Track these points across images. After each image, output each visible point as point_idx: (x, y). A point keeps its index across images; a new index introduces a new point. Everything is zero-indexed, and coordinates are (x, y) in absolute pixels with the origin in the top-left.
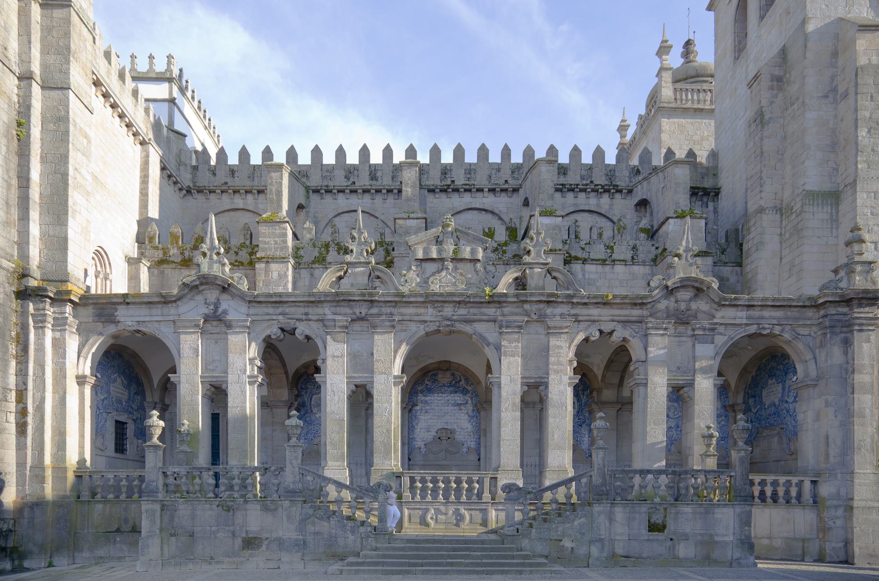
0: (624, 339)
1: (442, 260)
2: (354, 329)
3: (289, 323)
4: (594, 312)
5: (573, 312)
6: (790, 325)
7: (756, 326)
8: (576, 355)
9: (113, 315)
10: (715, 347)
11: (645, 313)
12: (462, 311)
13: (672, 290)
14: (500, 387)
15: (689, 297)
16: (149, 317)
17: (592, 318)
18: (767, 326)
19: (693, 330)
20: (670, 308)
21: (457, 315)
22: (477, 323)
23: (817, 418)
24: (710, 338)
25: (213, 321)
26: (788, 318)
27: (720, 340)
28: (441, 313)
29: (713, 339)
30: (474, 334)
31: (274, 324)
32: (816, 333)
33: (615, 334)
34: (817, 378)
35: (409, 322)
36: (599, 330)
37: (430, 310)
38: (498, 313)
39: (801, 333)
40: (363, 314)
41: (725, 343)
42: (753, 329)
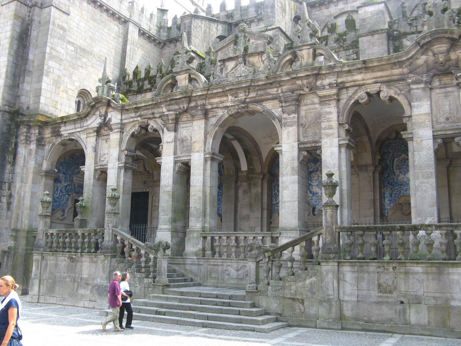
1: (237, 57)
2: (183, 120)
3: (144, 122)
4: (358, 77)
5: (340, 80)
9: (60, 132)
11: (405, 70)
12: (252, 95)
15: (446, 48)
16: (74, 130)
17: (357, 83)
20: (429, 62)
21: (249, 98)
25: (105, 127)
28: (237, 99)
30: (264, 111)
33: (382, 95)
35: (217, 110)
37: (230, 97)
38: (280, 91)
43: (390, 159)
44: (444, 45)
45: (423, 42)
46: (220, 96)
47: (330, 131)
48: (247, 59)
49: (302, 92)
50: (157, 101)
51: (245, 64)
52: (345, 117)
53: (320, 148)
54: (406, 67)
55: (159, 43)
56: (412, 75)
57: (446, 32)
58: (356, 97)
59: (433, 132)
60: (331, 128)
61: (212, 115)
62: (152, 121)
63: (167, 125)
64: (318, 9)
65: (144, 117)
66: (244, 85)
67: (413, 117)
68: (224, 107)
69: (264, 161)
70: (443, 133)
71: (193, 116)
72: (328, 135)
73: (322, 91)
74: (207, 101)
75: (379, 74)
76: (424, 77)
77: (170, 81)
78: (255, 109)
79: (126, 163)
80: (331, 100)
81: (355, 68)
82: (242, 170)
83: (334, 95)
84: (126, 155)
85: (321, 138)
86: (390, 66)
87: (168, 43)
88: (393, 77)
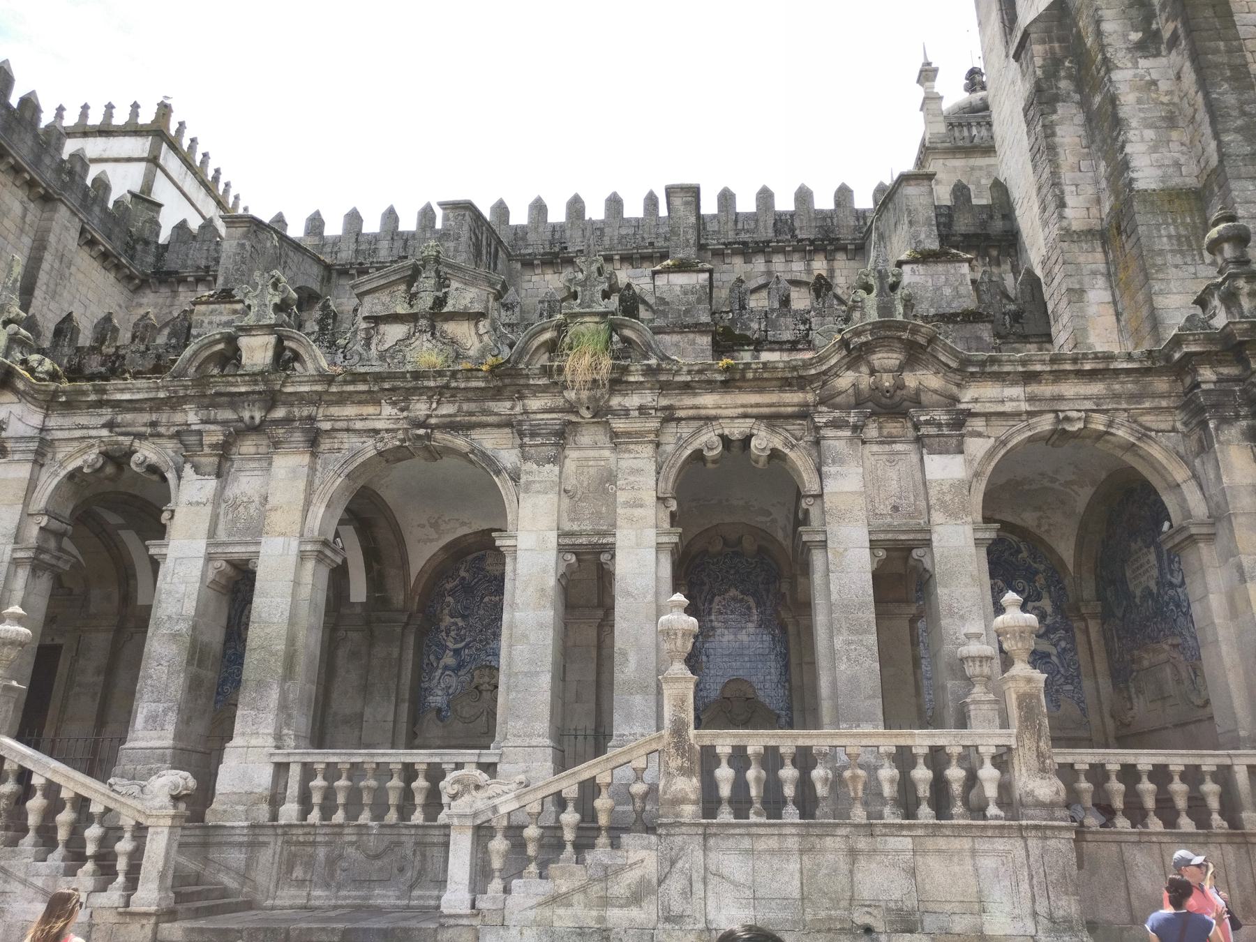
1: (412, 318)
2: (244, 449)
4: (708, 400)
5: (664, 402)
6: (1125, 410)
7: (1052, 416)
10: (969, 462)
11: (810, 397)
12: (447, 409)
14: (515, 559)
15: (898, 362)
17: (703, 412)
18: (1074, 414)
19: (916, 427)
20: (862, 387)
21: (437, 416)
22: (478, 431)
24: (954, 441)
26: (1116, 397)
27: (977, 447)
28: (405, 414)
30: (472, 452)
31: (93, 445)
32: (1185, 424)
33: (754, 442)
34: (1211, 520)
35: (345, 435)
36: (722, 436)
37: (388, 410)
38: (518, 409)
39: (1154, 426)
40: (257, 421)
41: (991, 453)
42: (1045, 424)
43: (703, 598)
44: (895, 356)
45: (857, 340)
46: (360, 403)
47: (638, 512)
48: (438, 325)
49: (574, 418)
50: (175, 392)
51: (433, 334)
52: (670, 484)
53: (610, 549)
55: (130, 278)
56: (824, 409)
57: (902, 326)
58: (697, 444)
59: (870, 533)
60: (637, 504)
61: (328, 446)
62: (146, 442)
63: (196, 459)
64: (537, 272)
65: (124, 429)
66: (432, 384)
67: (825, 497)
68: (365, 431)
69: (412, 582)
70: (890, 536)
71: (276, 444)
72: (630, 520)
73: (622, 421)
74: (321, 410)
76: (852, 415)
77: (221, 346)
78: (450, 445)
79: (39, 549)
80: (641, 443)
81: (703, 377)
82: (353, 599)
83: (649, 432)
84: (41, 528)
85: (614, 525)
86: (778, 383)
87: (155, 280)
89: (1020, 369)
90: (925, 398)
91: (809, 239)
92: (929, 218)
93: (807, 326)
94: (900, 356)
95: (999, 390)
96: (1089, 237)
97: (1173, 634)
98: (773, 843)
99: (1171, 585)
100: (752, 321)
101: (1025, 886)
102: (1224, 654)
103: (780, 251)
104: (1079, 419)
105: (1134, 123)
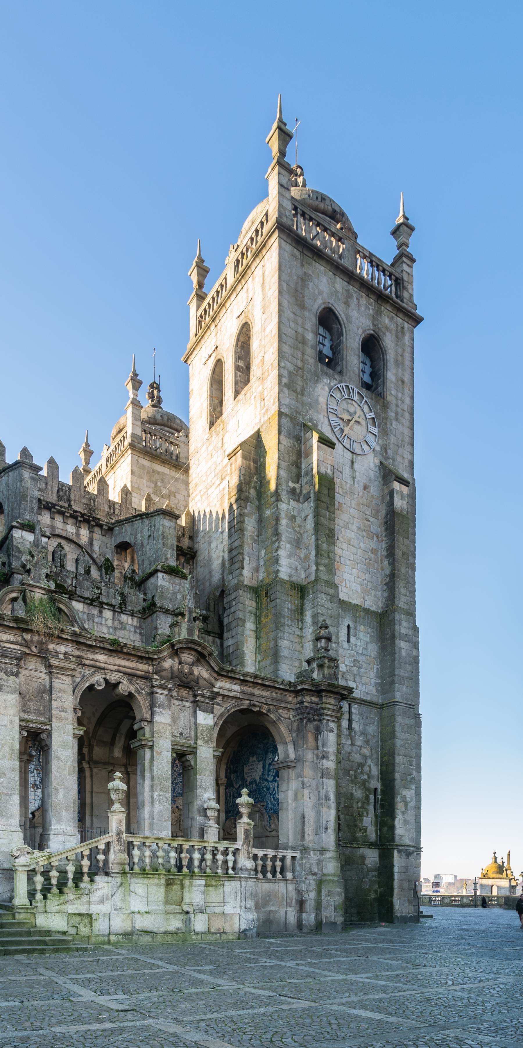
0: (130, 693)
7: (248, 702)
8: (80, 703)
11: (151, 669)
13: (177, 650)
15: (192, 660)
18: (257, 703)
19: (195, 696)
23: (296, 799)
24: (210, 706)
29: (213, 708)
36: (105, 679)
44: (192, 657)
54: (153, 665)
58: (94, 680)
75: (124, 663)
88: (137, 672)
89: (242, 678)
90: (201, 682)
91: (81, 513)
92: (173, 545)
93: (99, 592)
94: (194, 658)
95: (230, 685)
96: (252, 591)
97: (264, 801)
98: (156, 881)
99: (267, 780)
100: (68, 577)
101: (239, 897)
102: (289, 814)
103: (62, 513)
104: (258, 706)
105: (283, 539)
